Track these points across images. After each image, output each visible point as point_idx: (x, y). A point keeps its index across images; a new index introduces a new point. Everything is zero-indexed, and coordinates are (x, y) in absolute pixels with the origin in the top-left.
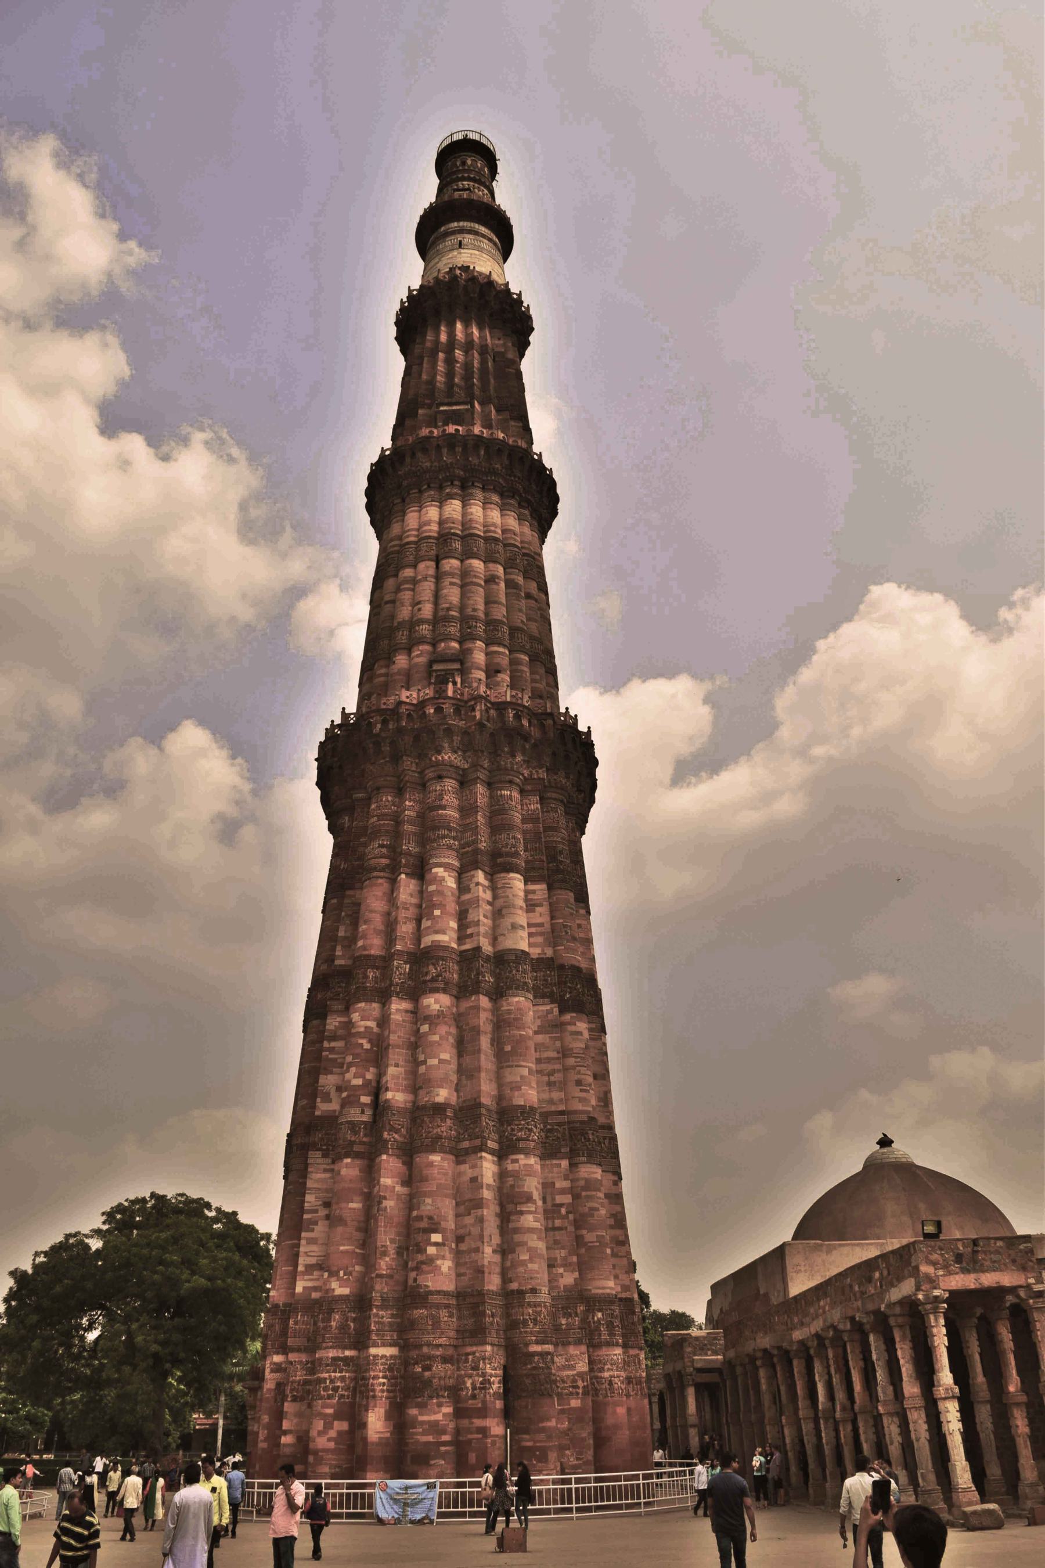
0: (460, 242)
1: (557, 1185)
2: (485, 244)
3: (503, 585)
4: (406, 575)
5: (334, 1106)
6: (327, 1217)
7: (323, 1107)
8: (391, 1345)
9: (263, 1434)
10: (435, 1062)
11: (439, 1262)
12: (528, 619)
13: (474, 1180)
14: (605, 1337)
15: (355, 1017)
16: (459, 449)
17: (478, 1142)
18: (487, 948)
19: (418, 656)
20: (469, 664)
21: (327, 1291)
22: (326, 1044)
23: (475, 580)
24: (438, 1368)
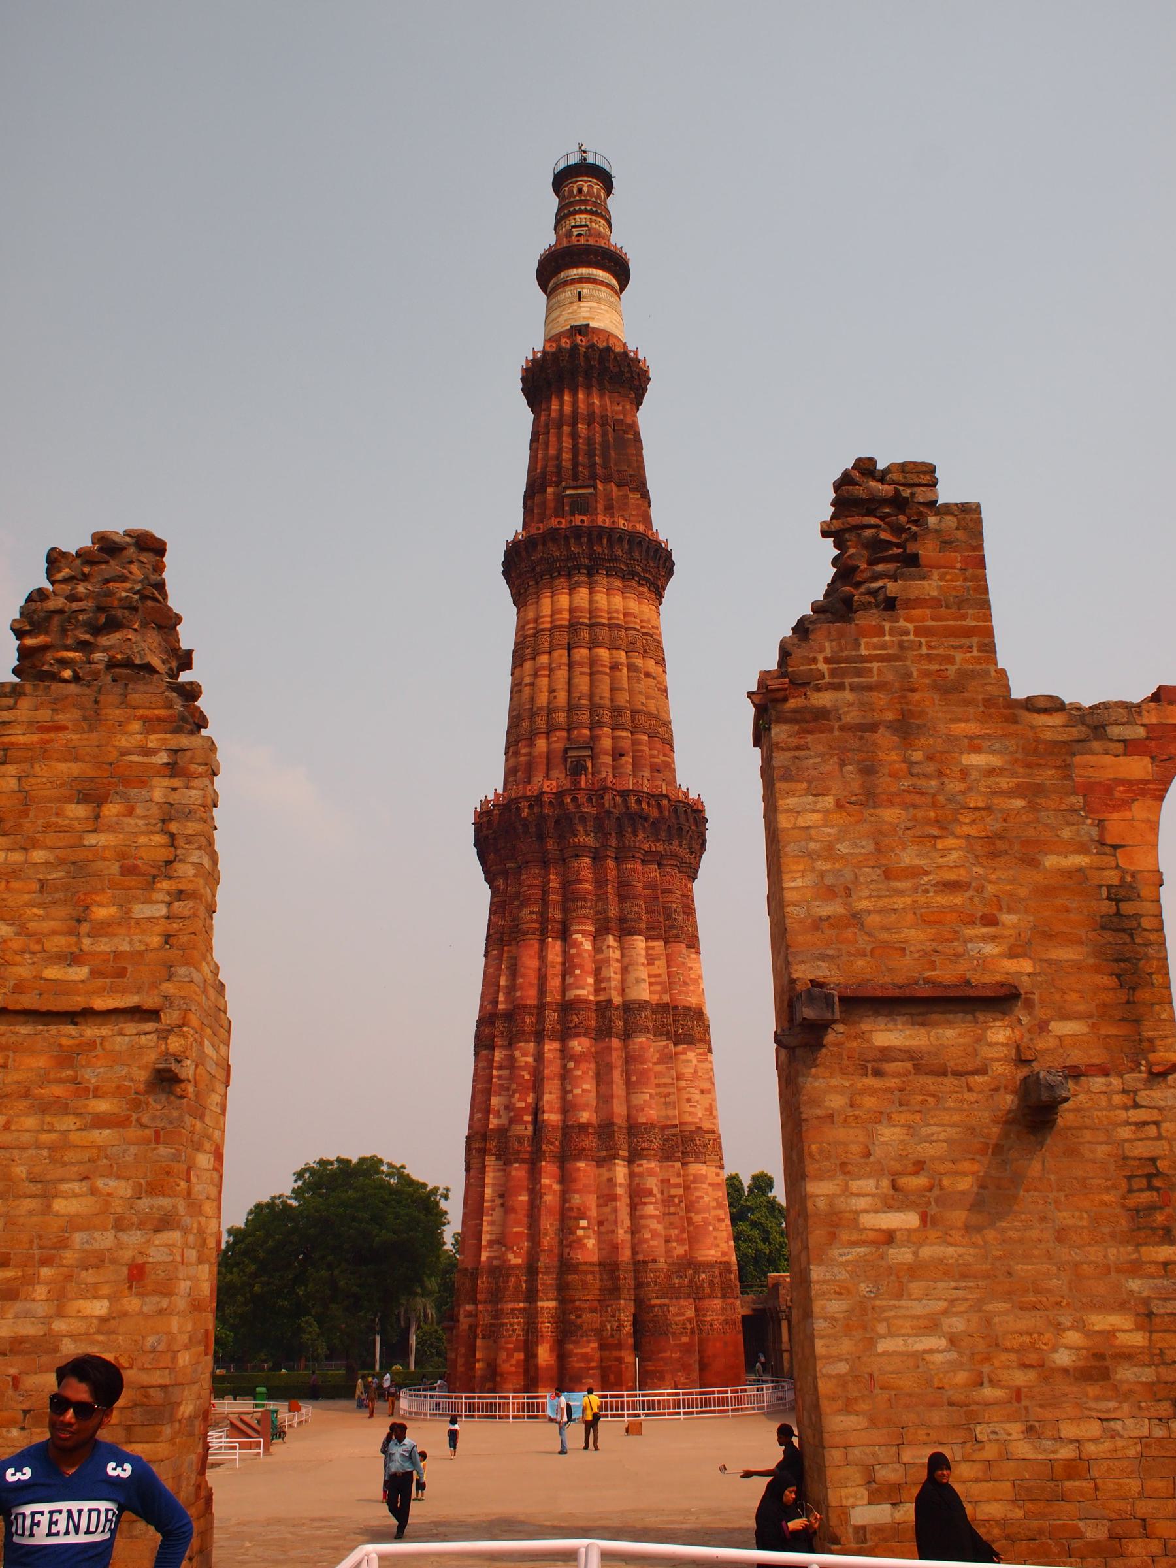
2: (604, 293)
3: (625, 670)
5: (504, 1121)
6: (502, 1205)
7: (494, 1122)
9: (461, 1361)
11: (586, 1241)
12: (648, 698)
13: (610, 1180)
14: (707, 1291)
15: (517, 1054)
16: (584, 540)
17: (612, 1152)
18: (617, 999)
19: (555, 742)
20: (597, 751)
22: (495, 1072)
23: (601, 669)
24: (587, 1316)
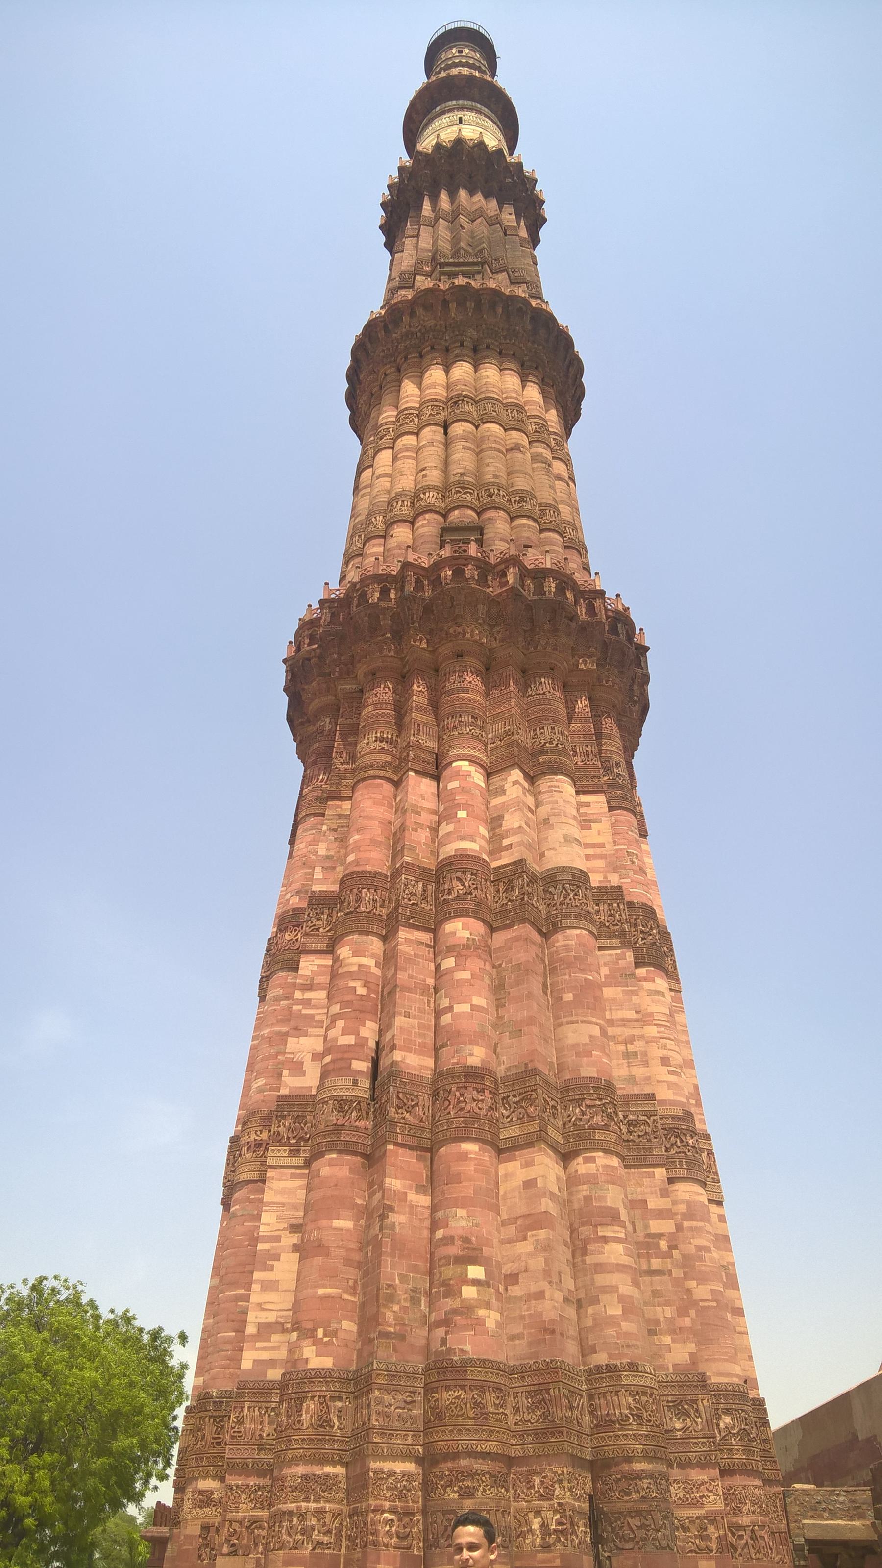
0: (460, 119)
1: (651, 1205)
3: (528, 455)
4: (404, 442)
5: (310, 1080)
6: (296, 1248)
7: (291, 1084)
8: (404, 1457)
10: (466, 1008)
11: (482, 1312)
15: (344, 952)
16: (471, 305)
20: (489, 534)
21: (295, 1363)
22: (298, 995)
23: (493, 445)
